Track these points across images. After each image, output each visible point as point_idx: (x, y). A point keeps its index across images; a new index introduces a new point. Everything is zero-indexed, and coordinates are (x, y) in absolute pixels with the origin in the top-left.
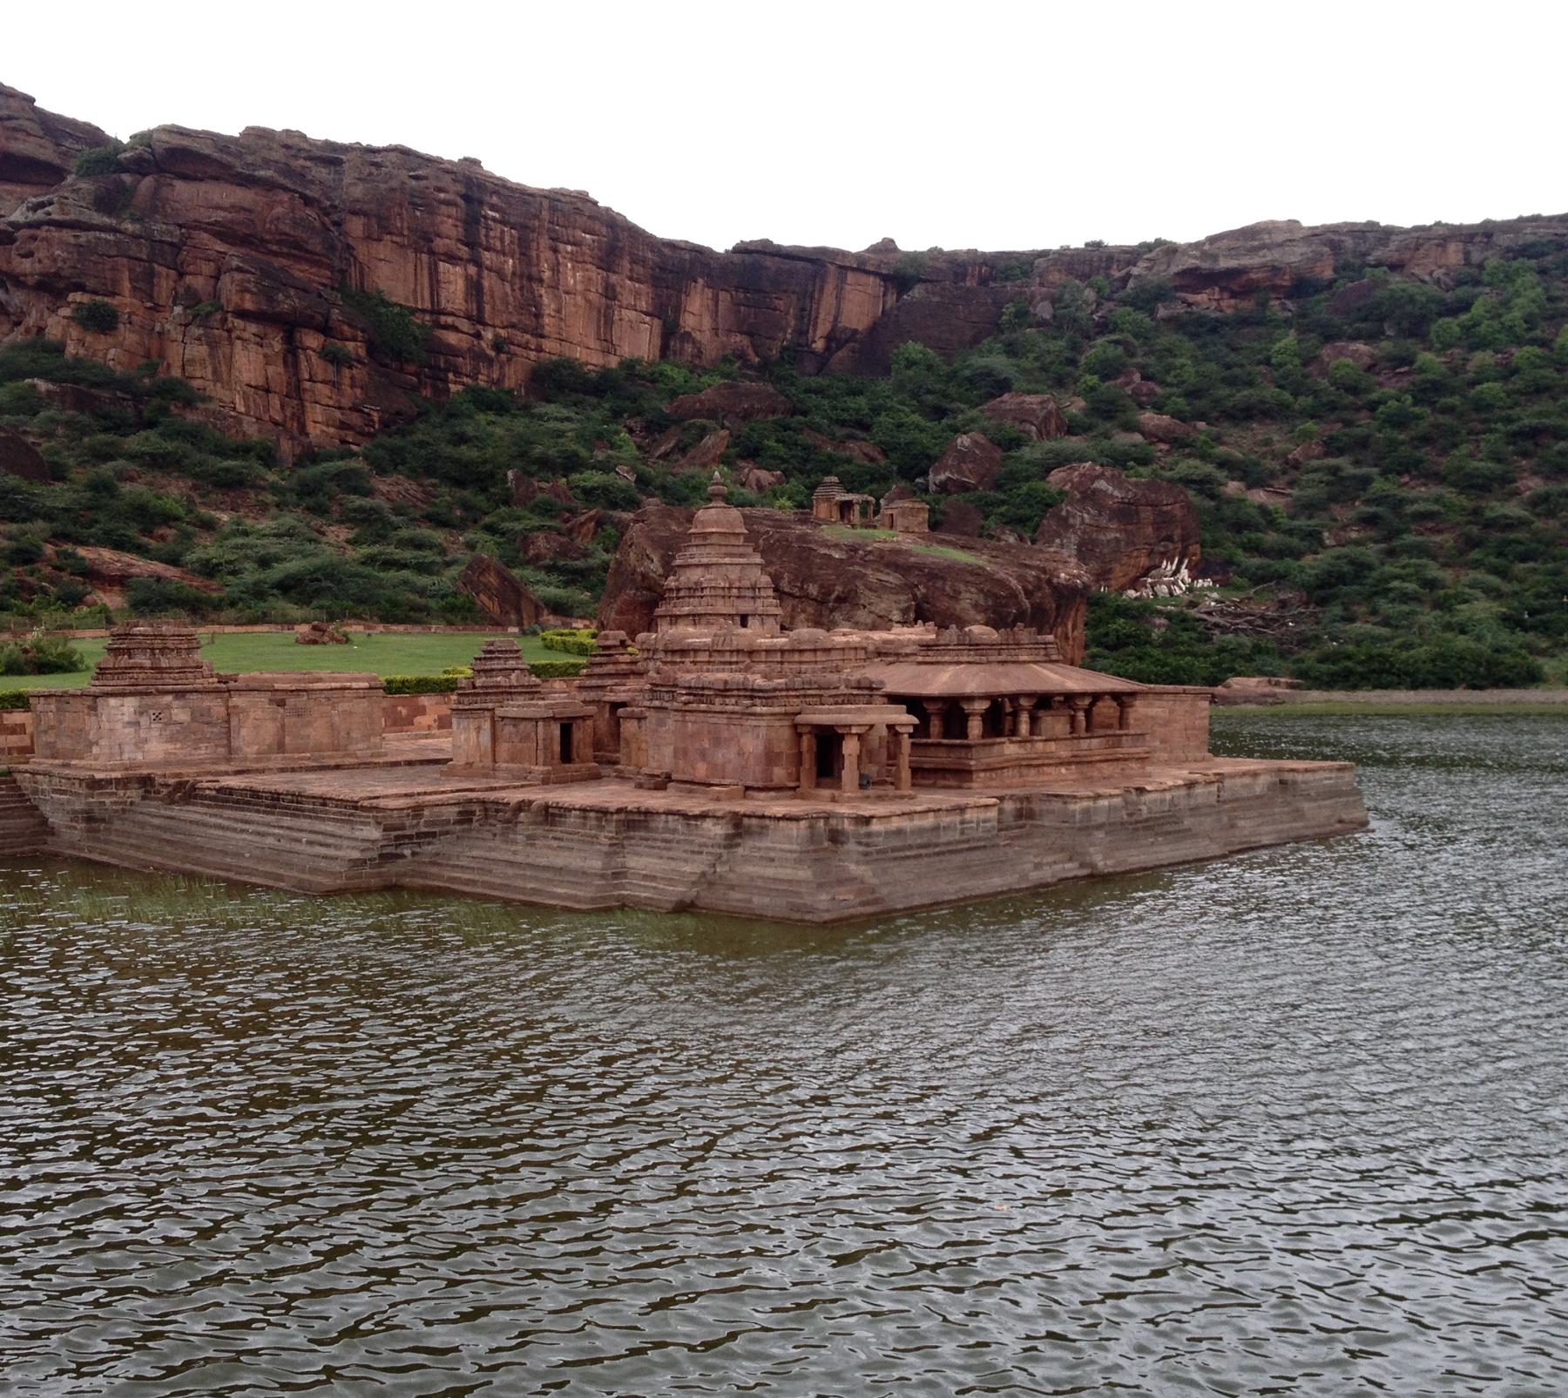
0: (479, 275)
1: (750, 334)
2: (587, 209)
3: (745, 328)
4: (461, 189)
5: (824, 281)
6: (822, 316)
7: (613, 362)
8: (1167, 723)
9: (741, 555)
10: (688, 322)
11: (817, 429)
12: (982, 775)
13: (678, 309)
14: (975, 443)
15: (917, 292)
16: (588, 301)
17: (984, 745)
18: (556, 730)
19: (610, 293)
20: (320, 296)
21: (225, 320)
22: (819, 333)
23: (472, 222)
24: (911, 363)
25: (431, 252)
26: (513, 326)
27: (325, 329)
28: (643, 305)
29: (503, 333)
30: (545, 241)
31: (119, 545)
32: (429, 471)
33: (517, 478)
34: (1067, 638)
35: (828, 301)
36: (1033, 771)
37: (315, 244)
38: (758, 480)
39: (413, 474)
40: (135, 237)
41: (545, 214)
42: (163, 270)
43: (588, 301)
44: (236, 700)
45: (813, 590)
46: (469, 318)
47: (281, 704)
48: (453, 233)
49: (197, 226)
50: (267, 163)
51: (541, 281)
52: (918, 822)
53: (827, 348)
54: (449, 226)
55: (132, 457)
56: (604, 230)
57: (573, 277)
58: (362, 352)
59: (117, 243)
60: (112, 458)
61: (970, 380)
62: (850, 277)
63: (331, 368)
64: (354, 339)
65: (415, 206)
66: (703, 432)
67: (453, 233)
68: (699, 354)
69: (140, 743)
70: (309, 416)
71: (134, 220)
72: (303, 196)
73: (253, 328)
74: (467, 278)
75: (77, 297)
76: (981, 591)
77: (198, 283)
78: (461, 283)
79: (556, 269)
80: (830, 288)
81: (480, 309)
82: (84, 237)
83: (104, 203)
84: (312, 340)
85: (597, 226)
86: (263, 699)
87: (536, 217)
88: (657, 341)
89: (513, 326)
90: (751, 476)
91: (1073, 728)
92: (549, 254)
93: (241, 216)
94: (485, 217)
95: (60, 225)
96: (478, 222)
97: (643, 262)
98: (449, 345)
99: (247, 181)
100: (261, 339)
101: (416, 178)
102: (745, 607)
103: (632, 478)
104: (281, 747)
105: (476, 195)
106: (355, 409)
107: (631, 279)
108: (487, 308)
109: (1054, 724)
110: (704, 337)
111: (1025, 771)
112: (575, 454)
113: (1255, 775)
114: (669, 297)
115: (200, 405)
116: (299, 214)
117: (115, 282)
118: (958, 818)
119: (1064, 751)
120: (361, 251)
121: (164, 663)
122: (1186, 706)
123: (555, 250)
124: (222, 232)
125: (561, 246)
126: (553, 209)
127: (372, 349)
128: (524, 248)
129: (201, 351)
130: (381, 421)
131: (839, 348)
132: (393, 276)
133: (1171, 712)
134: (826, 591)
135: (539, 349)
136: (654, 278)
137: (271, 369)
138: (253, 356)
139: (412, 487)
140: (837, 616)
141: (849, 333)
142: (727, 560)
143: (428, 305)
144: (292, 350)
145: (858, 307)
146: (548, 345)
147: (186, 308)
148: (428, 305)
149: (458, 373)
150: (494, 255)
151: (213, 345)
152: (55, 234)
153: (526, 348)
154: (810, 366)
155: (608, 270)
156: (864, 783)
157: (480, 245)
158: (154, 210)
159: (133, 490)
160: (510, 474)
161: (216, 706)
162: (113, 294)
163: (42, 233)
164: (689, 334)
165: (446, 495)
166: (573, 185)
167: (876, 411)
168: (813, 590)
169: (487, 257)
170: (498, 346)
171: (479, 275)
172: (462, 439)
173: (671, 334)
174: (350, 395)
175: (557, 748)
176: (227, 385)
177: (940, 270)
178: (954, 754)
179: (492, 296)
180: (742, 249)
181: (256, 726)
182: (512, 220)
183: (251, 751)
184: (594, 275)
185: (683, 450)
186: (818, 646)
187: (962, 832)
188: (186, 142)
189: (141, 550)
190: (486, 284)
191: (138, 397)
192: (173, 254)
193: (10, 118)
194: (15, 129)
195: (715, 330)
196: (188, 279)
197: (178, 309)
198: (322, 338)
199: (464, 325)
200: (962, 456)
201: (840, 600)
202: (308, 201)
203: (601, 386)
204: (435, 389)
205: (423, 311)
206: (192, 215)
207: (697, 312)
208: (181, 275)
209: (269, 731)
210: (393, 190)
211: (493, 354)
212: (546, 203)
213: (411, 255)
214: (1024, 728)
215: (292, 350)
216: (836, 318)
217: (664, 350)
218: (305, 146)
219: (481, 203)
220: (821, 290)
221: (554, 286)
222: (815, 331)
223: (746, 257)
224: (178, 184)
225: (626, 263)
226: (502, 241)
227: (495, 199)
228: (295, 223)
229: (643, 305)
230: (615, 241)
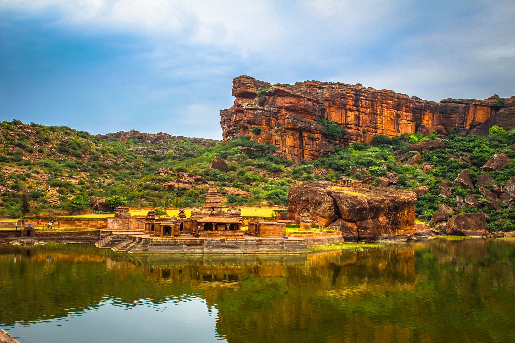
0: (359, 114)
1: (444, 125)
2: (391, 95)
3: (442, 123)
4: (353, 92)
5: (468, 109)
6: (469, 119)
7: (399, 135)
8: (274, 230)
10: (425, 122)
11: (452, 152)
13: (421, 120)
14: (499, 157)
15: (501, 110)
16: (391, 119)
18: (151, 226)
19: (398, 116)
20: (309, 123)
21: (285, 130)
22: (468, 124)
23: (357, 101)
24: (494, 132)
25: (346, 109)
26: (368, 127)
27: (310, 131)
28: (409, 119)
29: (365, 128)
30: (379, 104)
31: (237, 187)
32: (330, 166)
33: (352, 168)
34: (404, 215)
35: (471, 114)
37: (311, 110)
38: (426, 168)
39: (326, 168)
40: (267, 111)
41: (379, 97)
42: (273, 119)
43: (391, 119)
44: (130, 220)
45: (314, 201)
46: (355, 125)
47: (139, 221)
48: (351, 104)
49: (282, 108)
50: (299, 91)
51: (377, 114)
52: (164, 240)
53: (471, 128)
54: (350, 103)
55: (254, 165)
56: (396, 100)
57: (386, 113)
58: (320, 137)
59: (263, 113)
60: (248, 165)
61: (510, 136)
62: (478, 108)
63: (310, 141)
64: (317, 133)
65: (342, 98)
66: (413, 154)
67: (351, 104)
68: (428, 131)
69: (113, 226)
70: (305, 153)
71: (267, 107)
72: (307, 99)
73: (291, 132)
74: (355, 115)
75: (253, 126)
76: (348, 203)
77: (281, 121)
78: (353, 117)
79: (381, 111)
80: (471, 110)
81: (359, 123)
82: (256, 112)
83: (262, 103)
84: (306, 134)
86: (135, 220)
87: (376, 98)
88: (414, 128)
89: (368, 127)
90: (425, 167)
92: (380, 107)
93: (292, 105)
94: (361, 99)
96: (359, 100)
97: (409, 107)
98: (349, 133)
99: (294, 96)
100: (293, 135)
101: (342, 91)
102: (213, 206)
103: (386, 168)
104: (138, 228)
105: (358, 93)
106: (316, 151)
107: (406, 112)
108: (361, 123)
109: (219, 227)
110: (430, 126)
112: (372, 161)
113: (275, 240)
114: (418, 116)
115: (277, 151)
116: (306, 103)
117: (262, 122)
120: (328, 110)
121: (122, 213)
122: (280, 227)
123: (382, 106)
124: (287, 109)
125: (383, 105)
126: (380, 95)
127: (324, 135)
128: (372, 105)
129: (280, 138)
130: (323, 154)
131: (474, 128)
132: (335, 116)
134: (316, 201)
135: (376, 132)
136: (413, 111)
137: (295, 142)
138: (291, 139)
139: (324, 171)
140: (318, 208)
141: (478, 123)
143: (344, 122)
144: (301, 137)
145: (481, 116)
146: (378, 131)
147: (278, 127)
148: (344, 122)
149: (351, 140)
150: (364, 109)
151: (282, 136)
153: (372, 132)
154: (464, 133)
155: (398, 110)
156: (164, 235)
157: (359, 106)
158: (272, 104)
159: (247, 174)
160: (350, 167)
161: (127, 221)
162: (261, 125)
163: (248, 111)
164: (424, 126)
165: (332, 172)
166: (387, 88)
167: (475, 147)
168: (314, 201)
169: (362, 109)
170: (364, 133)
171: (359, 114)
172: (342, 158)
173: (418, 128)
174: (316, 147)
175: (151, 229)
176: (285, 146)
177: (510, 104)
179: (363, 119)
180: (441, 102)
181: (134, 224)
182: (369, 99)
183: (132, 228)
184: (393, 112)
185: (406, 159)
188: (280, 88)
189: (242, 188)
190: (361, 116)
191: (263, 150)
192: (276, 115)
193: (247, 84)
194: (249, 86)
195: (433, 124)
196: (279, 121)
197: (276, 128)
198: (309, 133)
199: (354, 127)
200: (494, 160)
201: (319, 204)
202: (309, 100)
203: (393, 142)
204: (345, 144)
205: (343, 124)
206: (280, 105)
207: (427, 120)
208: (277, 120)
209: (136, 225)
210: (336, 94)
211: (362, 134)
212: (379, 94)
213: (340, 110)
215: (301, 137)
216: (474, 119)
217: (416, 131)
218: (316, 85)
219: (360, 96)
220: (468, 112)
221: (381, 115)
222: (466, 123)
223: (443, 104)
224: (279, 98)
225: (404, 108)
226: (366, 105)
227: (364, 94)
228: (305, 106)
229: (409, 119)
230: (400, 102)
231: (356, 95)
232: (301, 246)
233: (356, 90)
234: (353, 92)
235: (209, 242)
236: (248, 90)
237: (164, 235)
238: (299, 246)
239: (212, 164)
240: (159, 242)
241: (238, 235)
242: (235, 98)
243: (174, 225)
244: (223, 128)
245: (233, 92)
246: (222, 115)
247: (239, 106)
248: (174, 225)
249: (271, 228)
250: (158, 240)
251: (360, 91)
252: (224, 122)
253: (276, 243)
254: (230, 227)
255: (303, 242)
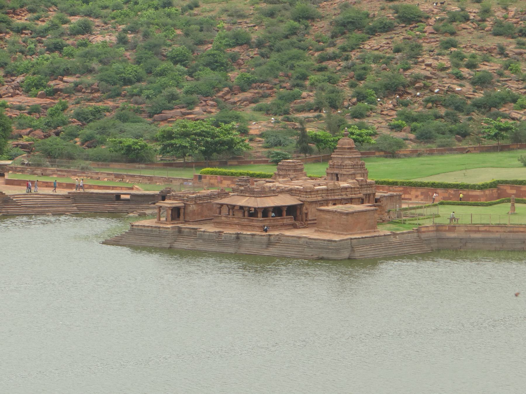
9: (341, 155)
52: (146, 228)
91: (244, 216)
102: (336, 171)
118: (158, 229)
133: (333, 218)
142: (335, 156)
187: (159, 233)
214: (231, 213)
232: (329, 249)
235: (201, 235)
237: (173, 219)
238: (326, 249)
240: (141, 230)
241: (254, 226)
243: (183, 205)
248: (183, 205)
249: (328, 216)
250: (140, 228)
253: (301, 242)
254: (263, 213)
255: (333, 244)
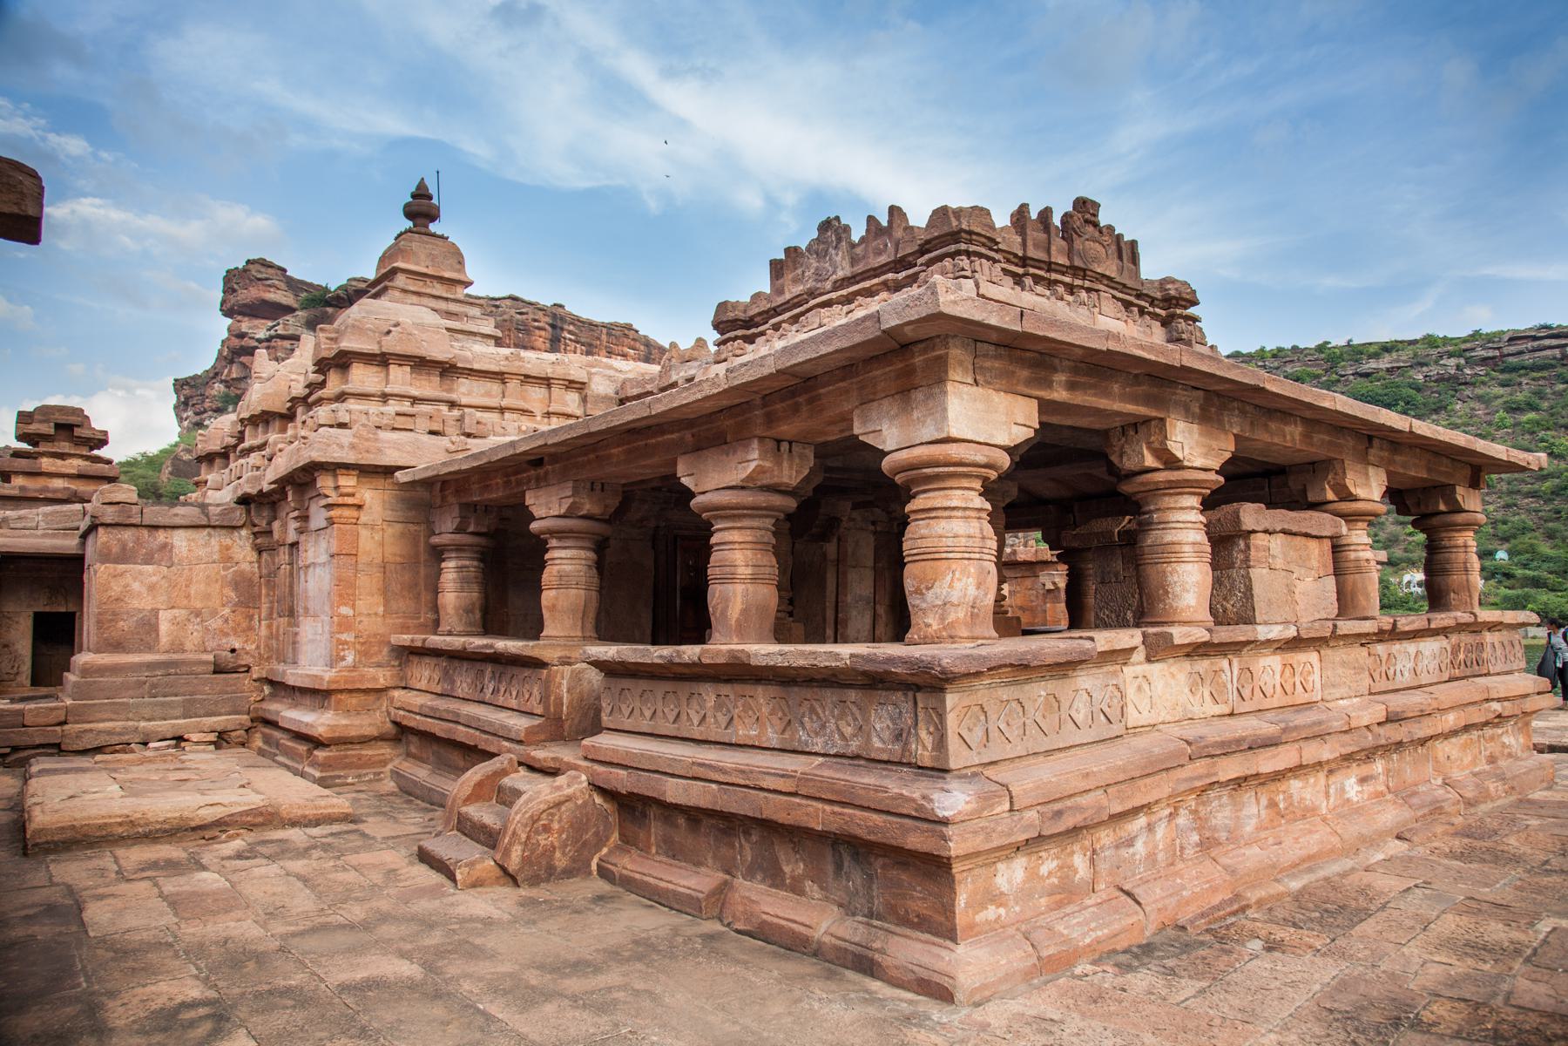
4: (548, 319)
12: (1011, 875)
17: (1022, 669)
36: (1253, 808)
41: (604, 337)
65: (519, 330)
85: (638, 345)
95: (283, 337)
105: (559, 324)
111: (1221, 812)
119: (1338, 686)
126: (609, 334)
152: (280, 343)
178: (831, 726)
186: (391, 345)
214: (1189, 583)
231: (553, 326)
233: (554, 316)
234: (548, 319)
236: (272, 296)
239: (173, 465)
242: (229, 321)
244: (180, 420)
245: (223, 302)
246: (177, 391)
247: (242, 336)
251: (562, 319)
252: (186, 404)
